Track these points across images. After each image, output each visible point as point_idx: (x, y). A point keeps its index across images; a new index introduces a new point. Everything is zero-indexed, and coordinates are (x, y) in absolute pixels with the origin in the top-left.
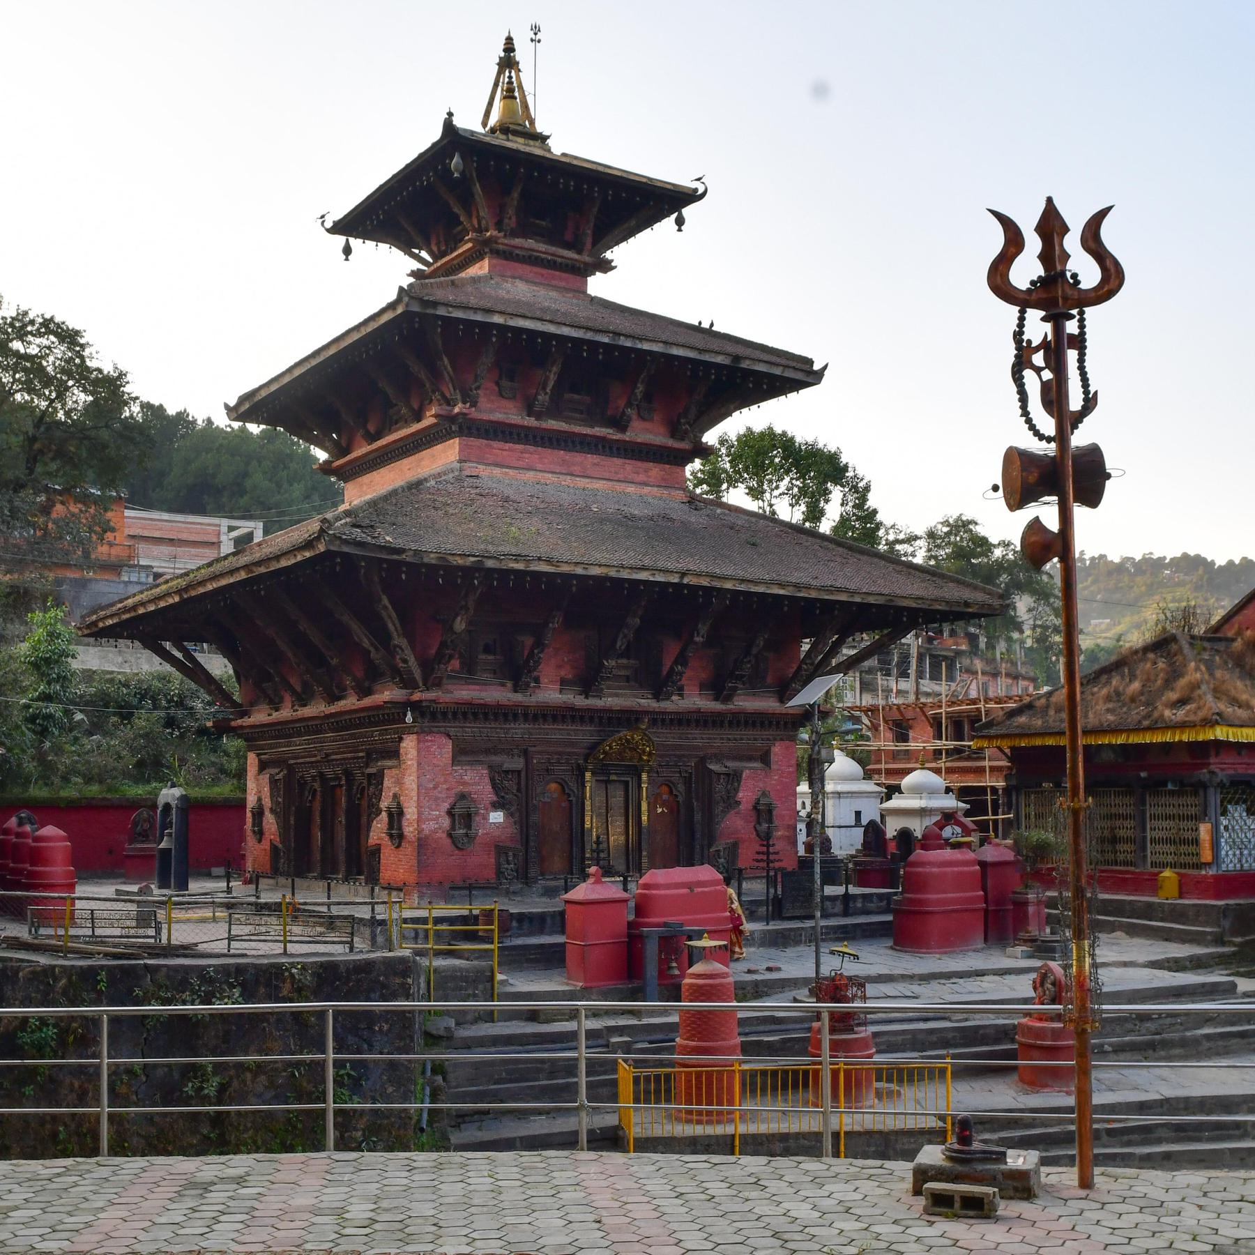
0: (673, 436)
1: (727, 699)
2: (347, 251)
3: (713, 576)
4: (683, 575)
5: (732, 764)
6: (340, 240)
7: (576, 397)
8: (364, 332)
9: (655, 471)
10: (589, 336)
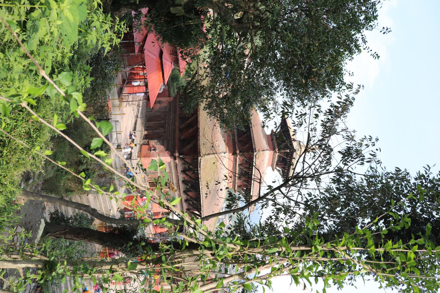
8: (252, 138)
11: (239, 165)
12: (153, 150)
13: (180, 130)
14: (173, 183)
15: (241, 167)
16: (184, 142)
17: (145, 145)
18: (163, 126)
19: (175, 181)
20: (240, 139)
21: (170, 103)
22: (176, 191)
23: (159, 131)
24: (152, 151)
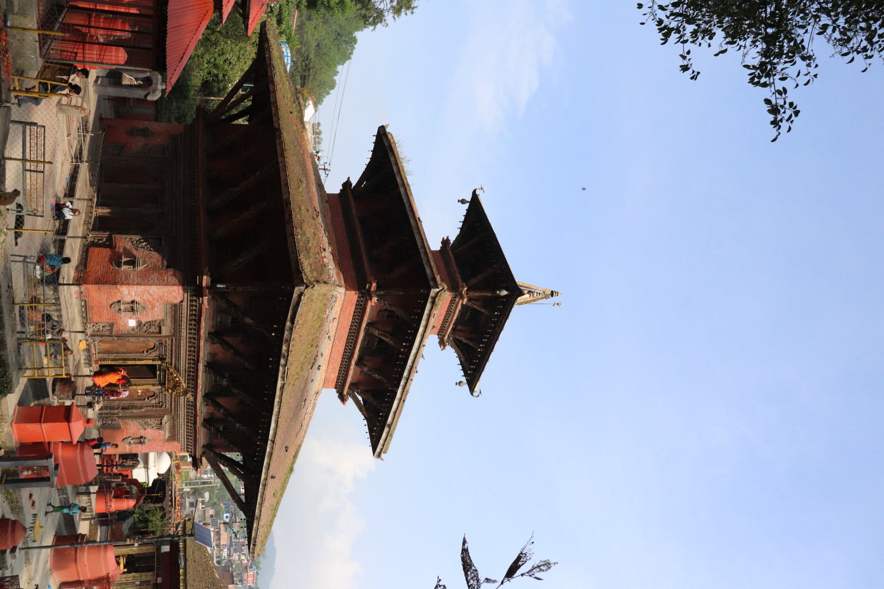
0: (351, 384)
1: (205, 427)
2: (463, 202)
3: (271, 454)
4: (273, 442)
5: (167, 426)
6: (469, 198)
8: (421, 251)
9: (334, 376)
11: (368, 325)
12: (126, 263)
14: (177, 369)
15: (371, 330)
17: (99, 246)
19: (183, 364)
22: (185, 393)
24: (124, 267)
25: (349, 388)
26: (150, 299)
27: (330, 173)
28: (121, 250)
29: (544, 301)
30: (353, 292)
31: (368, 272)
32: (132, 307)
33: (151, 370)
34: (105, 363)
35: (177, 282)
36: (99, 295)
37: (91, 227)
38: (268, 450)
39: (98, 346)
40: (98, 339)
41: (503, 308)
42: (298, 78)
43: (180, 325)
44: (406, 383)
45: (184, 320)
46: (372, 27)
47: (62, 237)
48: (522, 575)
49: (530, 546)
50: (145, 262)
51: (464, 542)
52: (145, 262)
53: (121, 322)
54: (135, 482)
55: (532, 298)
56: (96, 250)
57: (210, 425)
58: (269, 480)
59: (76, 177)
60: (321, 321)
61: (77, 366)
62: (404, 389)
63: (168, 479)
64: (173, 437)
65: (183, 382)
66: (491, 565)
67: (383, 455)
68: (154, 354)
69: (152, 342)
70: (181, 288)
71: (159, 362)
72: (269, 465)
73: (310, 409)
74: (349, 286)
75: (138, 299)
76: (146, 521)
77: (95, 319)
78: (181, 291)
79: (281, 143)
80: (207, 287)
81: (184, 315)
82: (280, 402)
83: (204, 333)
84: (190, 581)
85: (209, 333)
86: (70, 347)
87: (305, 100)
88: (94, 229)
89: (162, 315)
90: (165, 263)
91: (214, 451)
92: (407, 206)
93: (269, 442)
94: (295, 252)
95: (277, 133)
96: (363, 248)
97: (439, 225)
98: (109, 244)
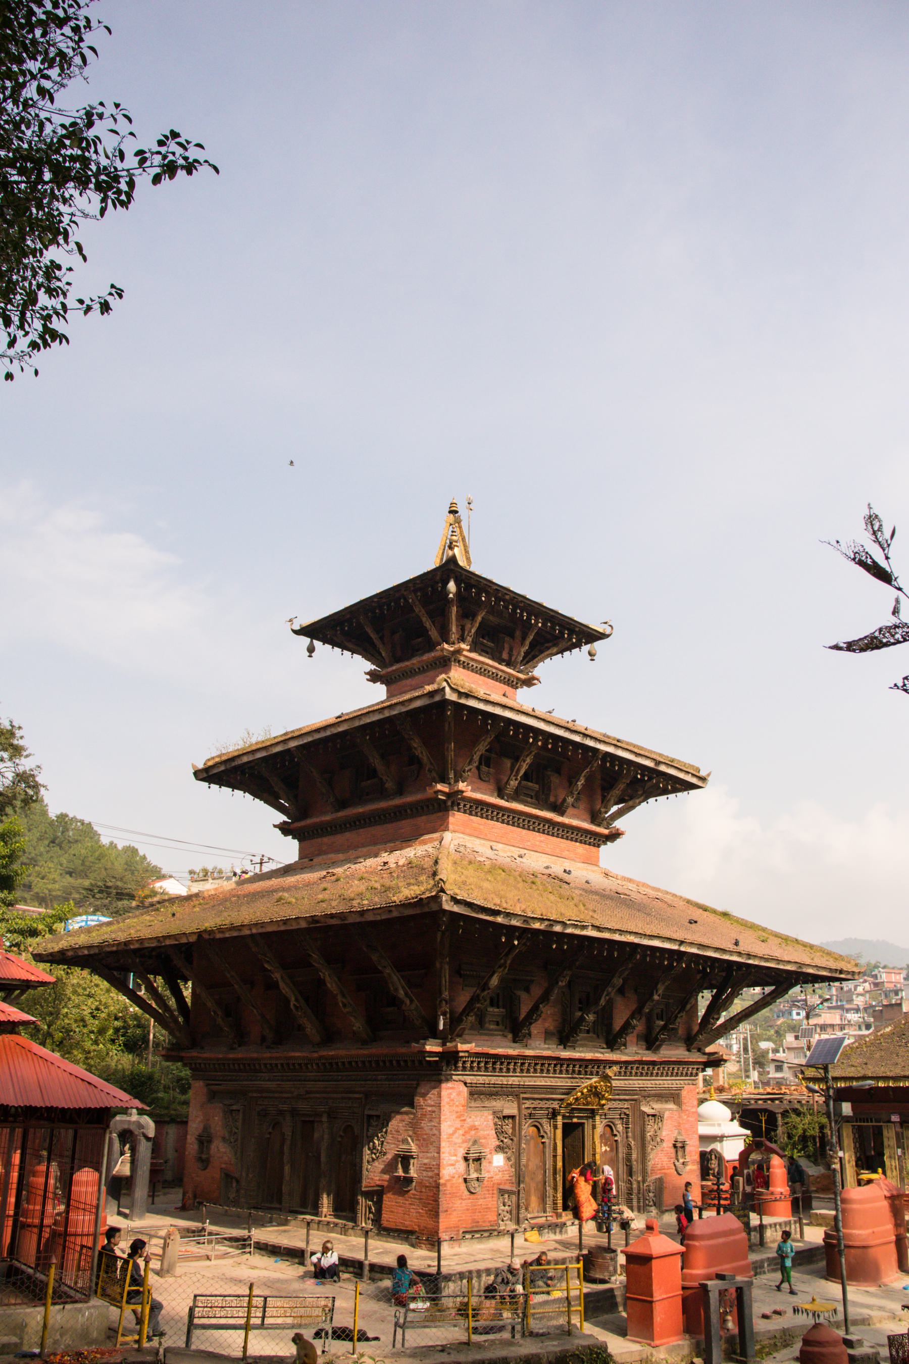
2: (311, 650)
3: (701, 946)
4: (682, 943)
5: (658, 1106)
6: (306, 641)
7: (530, 784)
8: (387, 714)
9: (580, 849)
10: (567, 735)
11: (501, 795)
12: (406, 1169)
13: (329, 1037)
14: (570, 1091)
15: (509, 791)
16: (384, 1018)
18: (308, 1125)
19: (561, 1081)
20: (389, 785)
21: (212, 1096)
22: (606, 1078)
23: (324, 1145)
24: (413, 1173)
25: (599, 825)
26: (462, 1132)
27: (267, 855)
28: (387, 1177)
29: (464, 524)
30: (451, 819)
31: (418, 797)
32: (474, 1160)
33: (569, 1129)
34: (560, 1202)
35: (435, 1091)
36: (455, 1210)
37: (351, 1224)
38: (694, 950)
39: (534, 1213)
40: (522, 1211)
41: (476, 589)
42: (120, 904)
43: (502, 1086)
44: (592, 738)
45: (493, 1080)
46: (42, 790)
47: (367, 1269)
48: (887, 558)
49: (843, 547)
50: (405, 1141)
51: (837, 647)
52: (405, 1141)
53: (498, 1178)
54: (744, 1155)
55: (460, 544)
56: (385, 1216)
57: (656, 1039)
58: (740, 949)
59: (274, 1246)
60: (496, 869)
61: (566, 1245)
62: (600, 741)
63: (738, 1104)
64: (674, 1097)
65: (589, 1082)
66: (872, 607)
67: (703, 773)
68: (547, 1127)
69: (528, 1129)
70: (444, 1085)
71: (559, 1118)
72: (717, 949)
73: (632, 886)
74: (442, 826)
75: (461, 1152)
76: (804, 1138)
77: (492, 1217)
78: (450, 1085)
79: (220, 930)
80: (444, 1044)
81: (487, 1080)
82: (621, 932)
83: (514, 1048)
84: (898, 1071)
85: (515, 1041)
86: (535, 1256)
87: (154, 893)
88: (354, 1219)
89: (486, 1113)
90: (405, 1109)
91: (696, 1035)
92: (317, 736)
93: (683, 949)
94: (388, 909)
95: (206, 936)
96: (382, 804)
97: (346, 687)
98: (377, 1195)
